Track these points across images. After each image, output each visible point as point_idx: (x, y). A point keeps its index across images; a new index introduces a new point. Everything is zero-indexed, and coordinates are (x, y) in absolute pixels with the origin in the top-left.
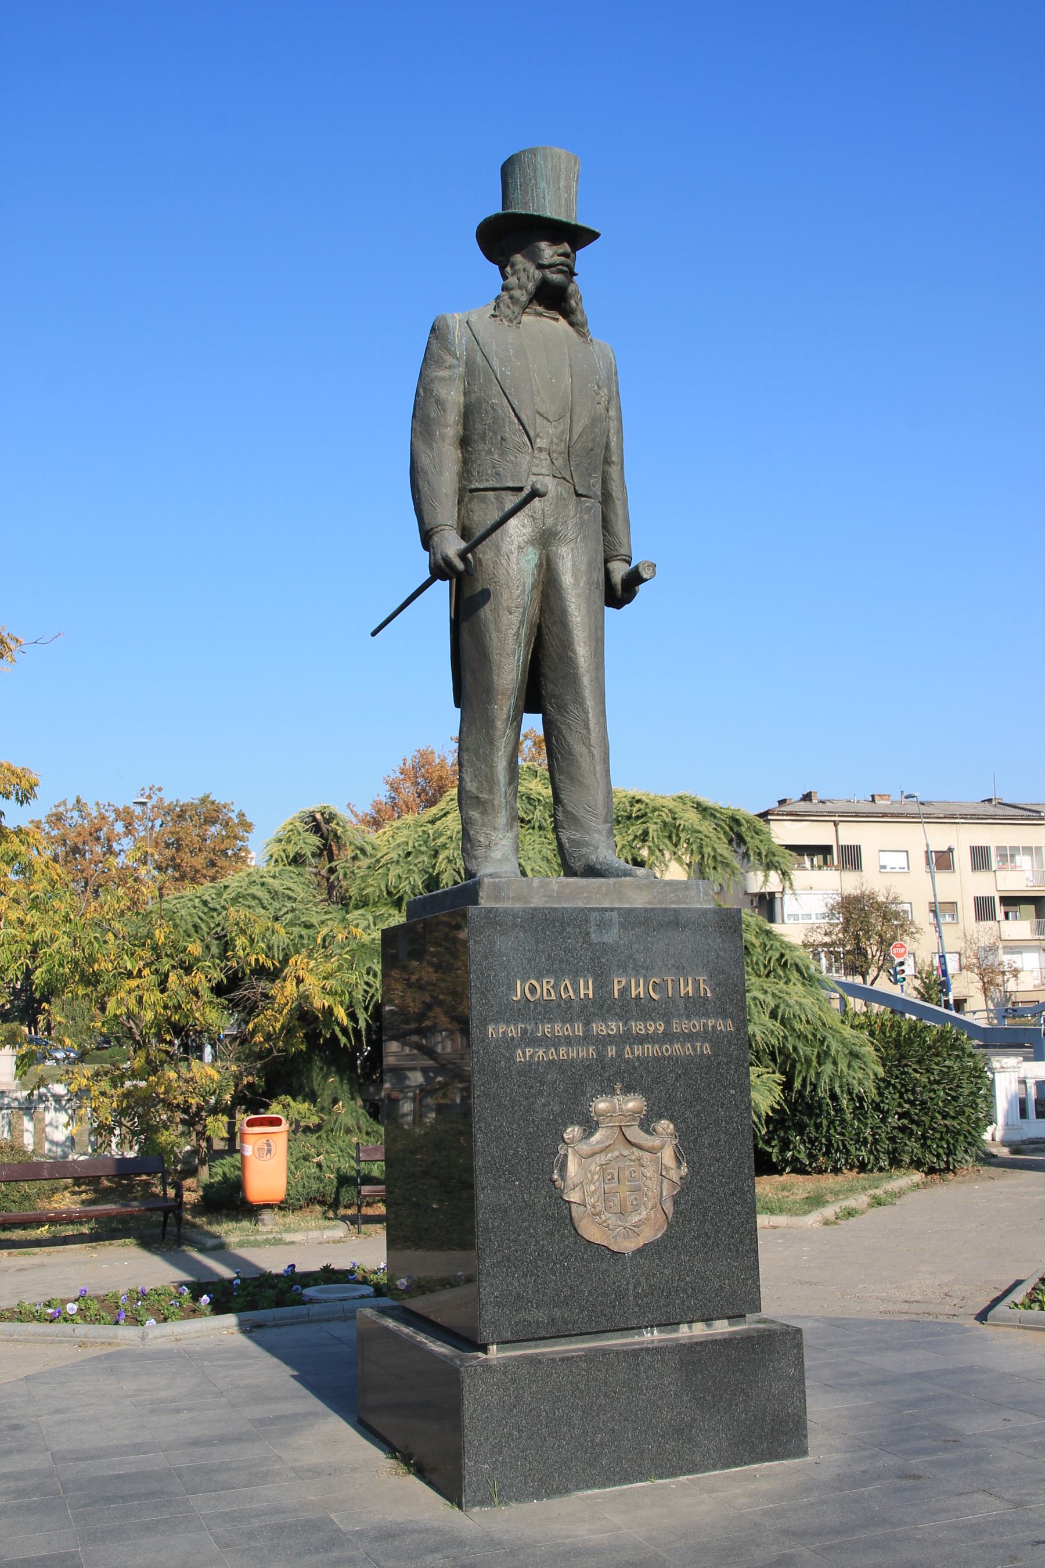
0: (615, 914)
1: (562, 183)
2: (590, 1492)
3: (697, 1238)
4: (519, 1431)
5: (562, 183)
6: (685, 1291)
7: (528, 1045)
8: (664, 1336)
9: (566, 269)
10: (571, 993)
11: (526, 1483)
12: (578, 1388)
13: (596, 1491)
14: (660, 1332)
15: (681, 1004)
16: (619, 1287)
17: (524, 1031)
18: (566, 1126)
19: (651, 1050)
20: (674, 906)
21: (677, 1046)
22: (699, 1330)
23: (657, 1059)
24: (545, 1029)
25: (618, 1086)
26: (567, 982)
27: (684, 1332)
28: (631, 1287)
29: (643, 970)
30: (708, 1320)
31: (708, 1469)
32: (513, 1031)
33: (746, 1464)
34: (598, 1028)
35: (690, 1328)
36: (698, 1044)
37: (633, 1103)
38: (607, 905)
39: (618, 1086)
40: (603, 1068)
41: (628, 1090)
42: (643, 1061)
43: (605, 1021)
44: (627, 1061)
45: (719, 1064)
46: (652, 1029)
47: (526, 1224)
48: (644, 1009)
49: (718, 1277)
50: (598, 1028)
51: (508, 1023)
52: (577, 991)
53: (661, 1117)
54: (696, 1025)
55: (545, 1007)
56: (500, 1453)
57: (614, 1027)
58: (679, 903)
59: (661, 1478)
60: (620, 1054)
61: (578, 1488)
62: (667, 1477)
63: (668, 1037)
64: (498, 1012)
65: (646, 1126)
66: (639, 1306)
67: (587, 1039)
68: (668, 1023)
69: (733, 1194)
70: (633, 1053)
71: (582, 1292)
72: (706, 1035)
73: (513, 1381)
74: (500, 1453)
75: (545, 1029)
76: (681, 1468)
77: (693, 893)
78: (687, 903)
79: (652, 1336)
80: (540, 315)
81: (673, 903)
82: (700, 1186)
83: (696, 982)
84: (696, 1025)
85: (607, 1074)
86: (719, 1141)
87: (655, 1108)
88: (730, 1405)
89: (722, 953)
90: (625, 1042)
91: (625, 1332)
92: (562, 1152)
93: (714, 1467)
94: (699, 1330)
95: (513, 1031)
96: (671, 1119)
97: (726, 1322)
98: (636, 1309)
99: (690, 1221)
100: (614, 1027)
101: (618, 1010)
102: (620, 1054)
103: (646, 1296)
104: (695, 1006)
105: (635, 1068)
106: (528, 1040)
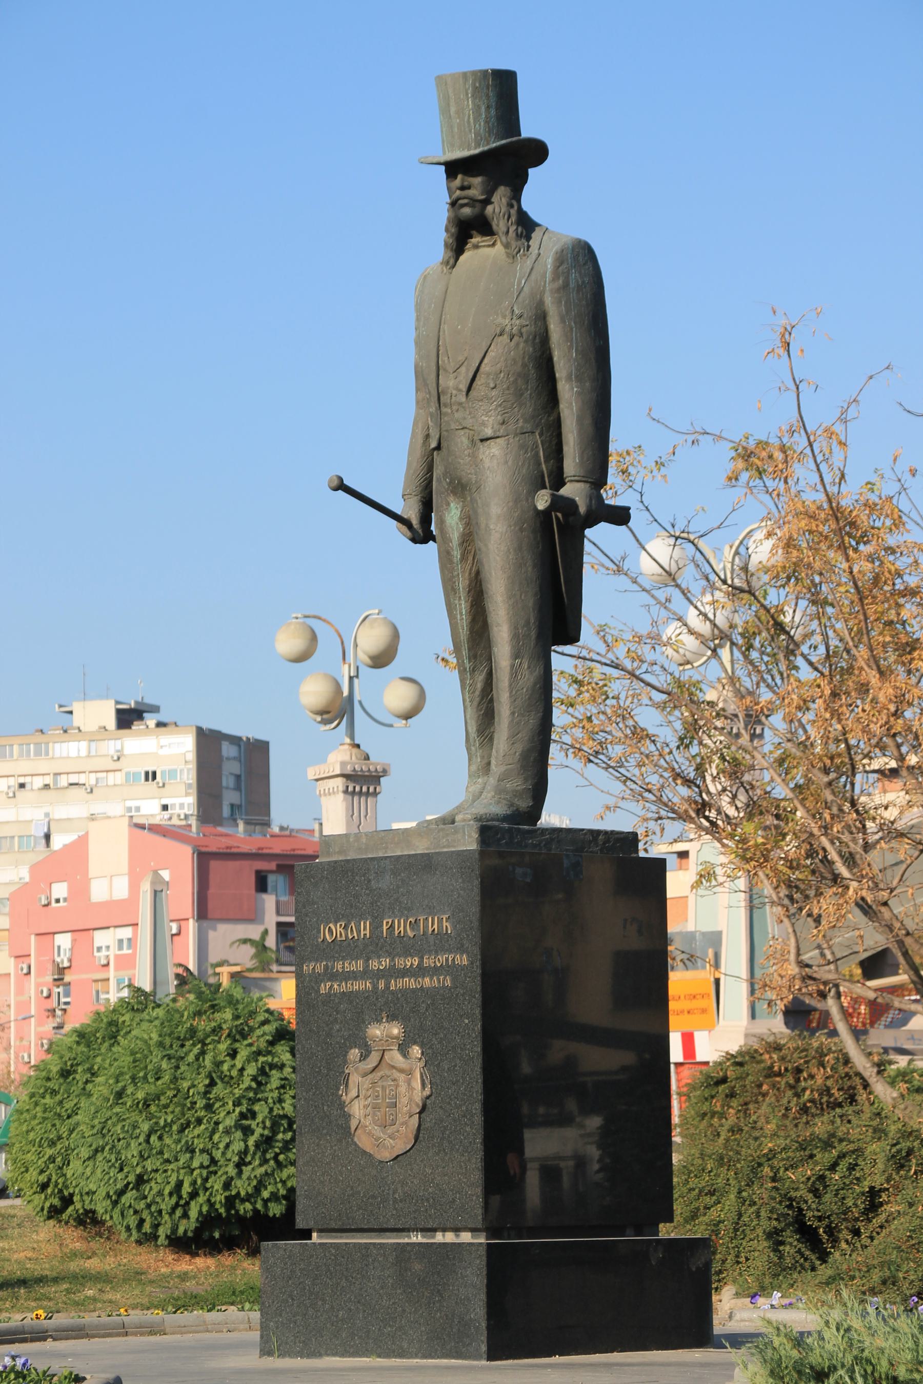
0: (387, 862)
1: (453, 109)
2: (334, 1359)
3: (438, 1154)
4: (293, 1299)
5: (453, 109)
6: (428, 1200)
7: (329, 980)
8: (425, 1241)
9: (466, 201)
10: (355, 934)
11: (295, 1343)
12: (329, 1270)
13: (338, 1359)
14: (423, 1237)
15: (431, 940)
16: (383, 1191)
17: (326, 967)
18: (351, 1048)
19: (410, 983)
20: (445, 850)
21: (427, 980)
22: (450, 1237)
23: (414, 991)
24: (339, 966)
25: (384, 1015)
26: (353, 924)
27: (439, 1238)
28: (391, 1192)
29: (404, 911)
30: (457, 1230)
31: (411, 1357)
32: (320, 968)
33: (438, 1358)
34: (374, 964)
35: (444, 1236)
36: (441, 978)
37: (396, 1030)
38: (381, 855)
39: (384, 1015)
40: (377, 999)
41: (392, 1018)
42: (405, 992)
43: (379, 957)
44: (393, 992)
45: (457, 995)
46: (409, 964)
47: (325, 1131)
48: (406, 947)
49: (452, 1190)
50: (374, 964)
51: (317, 961)
52: (359, 932)
53: (415, 1043)
54: (442, 959)
55: (340, 946)
56: (281, 1315)
57: (385, 962)
58: (448, 846)
59: (379, 1356)
60: (387, 986)
61: (328, 1355)
62: (384, 1357)
63: (421, 971)
64: (311, 952)
65: (403, 1049)
66: (396, 1209)
67: (365, 974)
68: (421, 958)
69: (464, 1116)
70: (396, 985)
71: (359, 1193)
72: (447, 969)
73: (289, 1257)
74: (281, 1315)
75: (339, 966)
76: (394, 1352)
77: (459, 836)
78: (454, 847)
79: (417, 1238)
80: (476, 247)
81: (444, 847)
82: (441, 1107)
83: (440, 921)
84: (442, 959)
85: (379, 1005)
86: (455, 1066)
87: (411, 1035)
88: (429, 1303)
89: (462, 892)
90: (392, 976)
91: (399, 1234)
92: (347, 1071)
93: (416, 1356)
94: (450, 1237)
95: (320, 968)
96: (421, 1047)
97: (469, 1234)
98: (394, 1212)
99: (433, 1137)
100: (385, 962)
101: (388, 948)
102: (387, 986)
103: (401, 1201)
104: (441, 942)
105: (398, 999)
106: (333, 976)
